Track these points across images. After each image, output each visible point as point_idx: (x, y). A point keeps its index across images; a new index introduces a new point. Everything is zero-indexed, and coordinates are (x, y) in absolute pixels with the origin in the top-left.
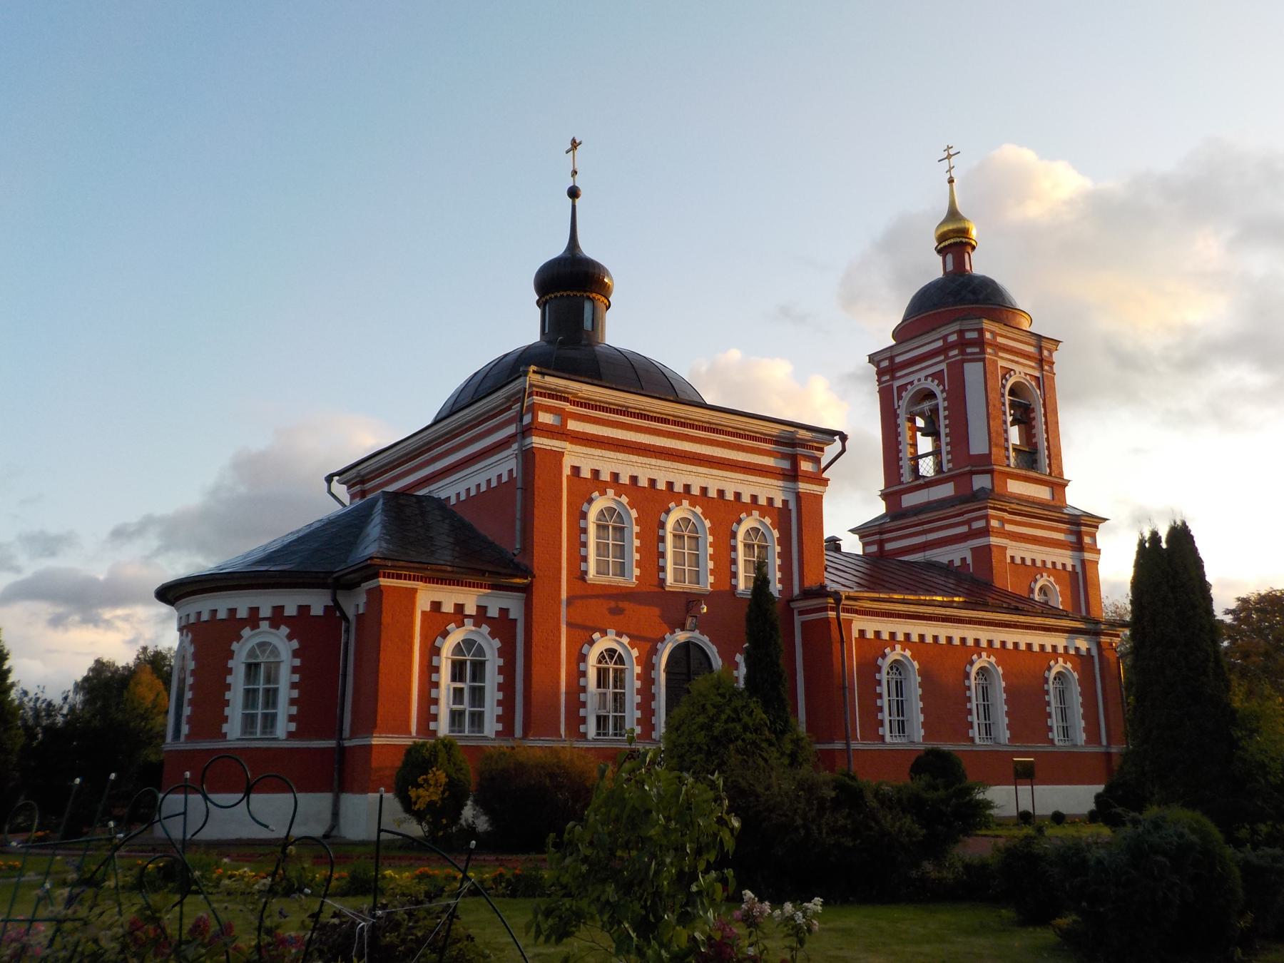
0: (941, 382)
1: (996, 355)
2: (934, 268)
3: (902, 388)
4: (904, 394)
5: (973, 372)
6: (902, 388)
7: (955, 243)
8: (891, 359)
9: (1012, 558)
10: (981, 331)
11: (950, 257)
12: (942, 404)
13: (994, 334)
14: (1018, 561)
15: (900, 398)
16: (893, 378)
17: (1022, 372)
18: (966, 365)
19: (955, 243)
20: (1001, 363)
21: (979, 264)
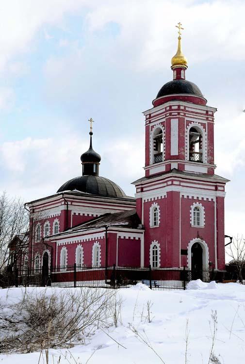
0: (164, 126)
1: (185, 115)
2: (169, 77)
3: (153, 127)
4: (153, 129)
5: (174, 123)
6: (153, 127)
7: (179, 68)
8: (150, 115)
9: (183, 196)
10: (179, 106)
11: (175, 71)
12: (164, 135)
13: (185, 107)
14: (185, 197)
15: (152, 130)
16: (150, 122)
17: (196, 123)
18: (172, 120)
19: (179, 68)
20: (186, 119)
21: (189, 76)
